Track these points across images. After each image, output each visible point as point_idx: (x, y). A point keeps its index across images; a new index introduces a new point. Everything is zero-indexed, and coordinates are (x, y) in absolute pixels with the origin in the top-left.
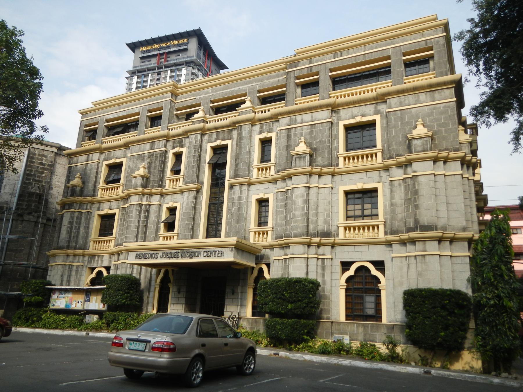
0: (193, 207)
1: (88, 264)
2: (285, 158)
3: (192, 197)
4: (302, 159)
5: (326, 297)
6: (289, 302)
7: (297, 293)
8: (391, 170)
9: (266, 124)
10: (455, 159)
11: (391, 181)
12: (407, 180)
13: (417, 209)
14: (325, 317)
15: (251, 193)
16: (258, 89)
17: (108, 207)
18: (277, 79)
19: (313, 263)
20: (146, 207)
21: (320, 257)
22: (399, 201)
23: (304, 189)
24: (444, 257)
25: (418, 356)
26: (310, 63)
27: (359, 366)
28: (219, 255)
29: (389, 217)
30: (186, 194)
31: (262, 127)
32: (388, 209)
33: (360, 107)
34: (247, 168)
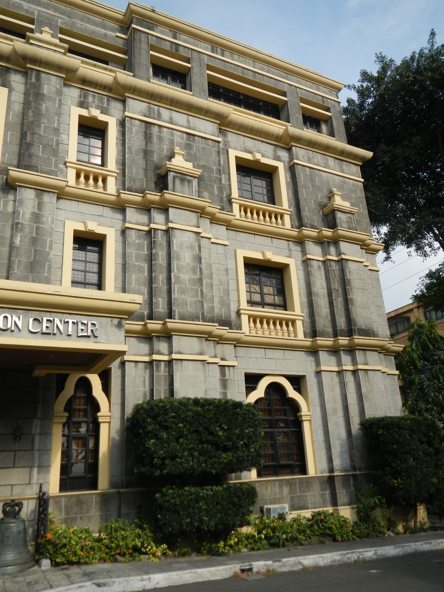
2: (141, 171)
4: (186, 183)
18: (104, 31)
26: (175, 37)
27: (388, 555)
31: (85, 97)
33: (256, 141)
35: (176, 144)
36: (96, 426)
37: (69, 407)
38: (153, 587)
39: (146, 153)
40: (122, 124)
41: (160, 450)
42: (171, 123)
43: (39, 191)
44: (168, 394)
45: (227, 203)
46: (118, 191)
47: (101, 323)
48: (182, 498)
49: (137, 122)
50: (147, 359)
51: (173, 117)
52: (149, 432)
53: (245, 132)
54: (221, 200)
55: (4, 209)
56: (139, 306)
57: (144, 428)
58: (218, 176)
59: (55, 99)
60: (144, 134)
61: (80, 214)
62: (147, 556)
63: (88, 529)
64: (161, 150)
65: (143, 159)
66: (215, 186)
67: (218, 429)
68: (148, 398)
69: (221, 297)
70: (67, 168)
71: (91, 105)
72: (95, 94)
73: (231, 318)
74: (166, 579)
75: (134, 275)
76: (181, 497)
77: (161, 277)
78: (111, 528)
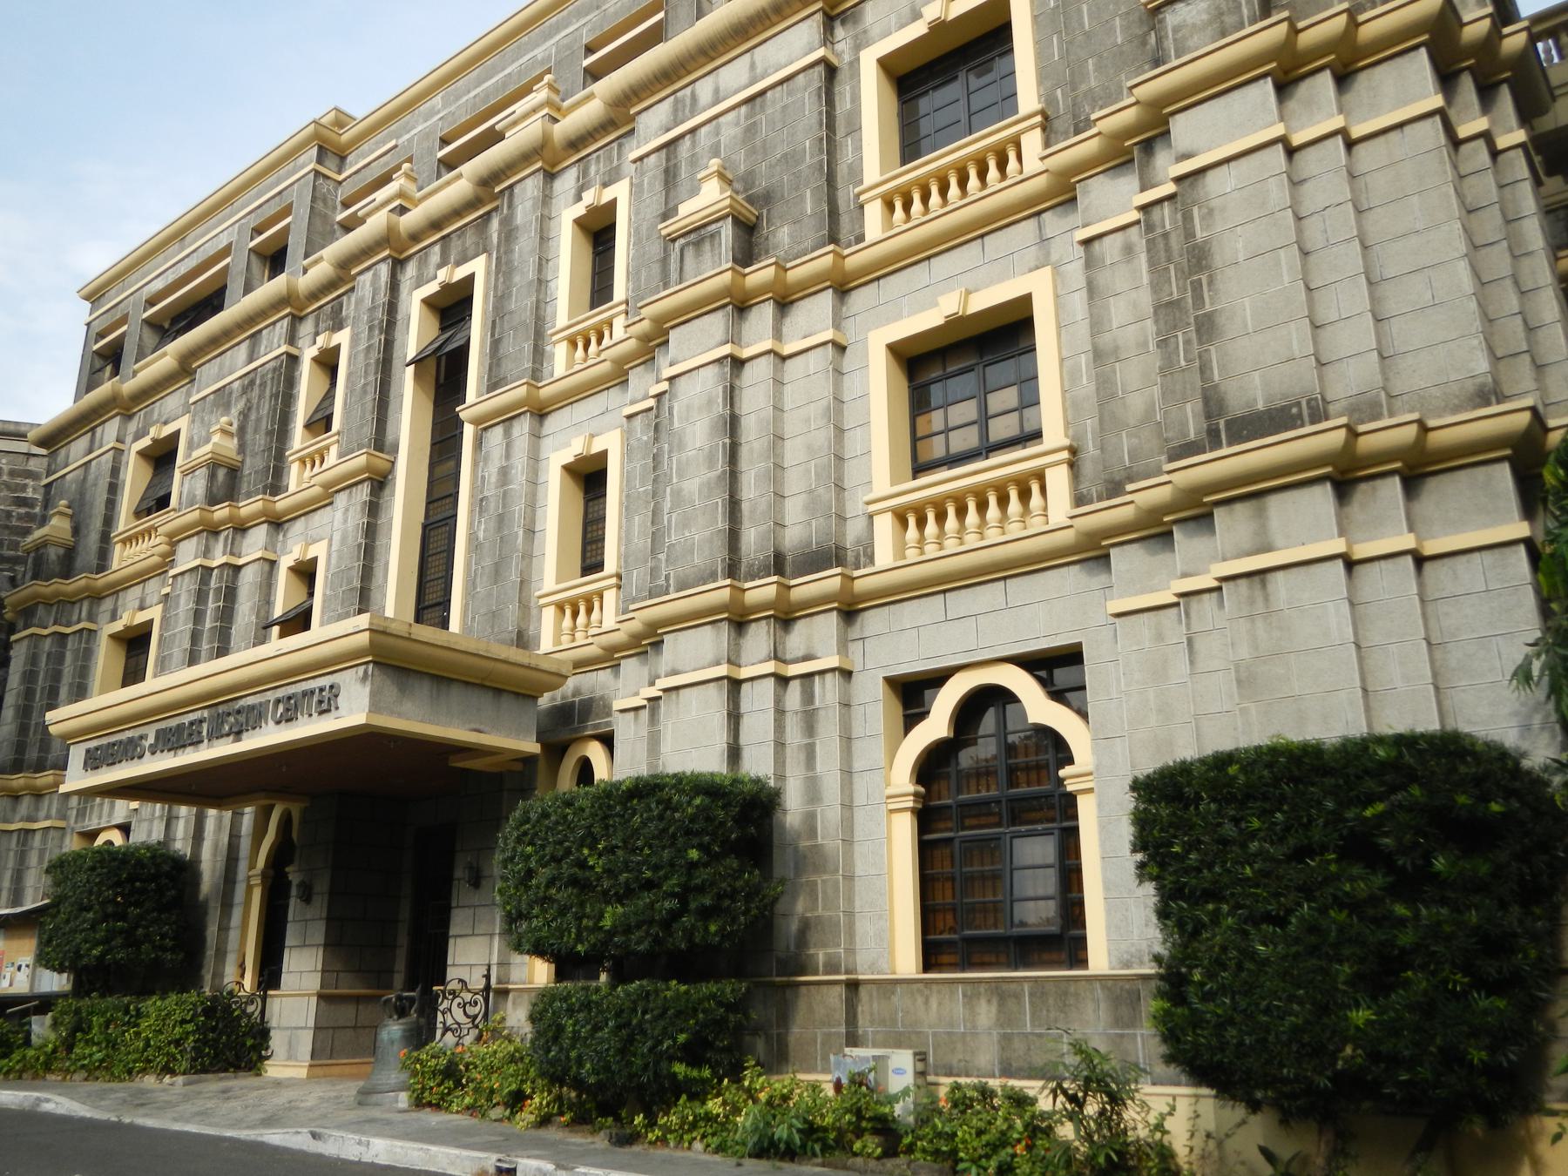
0: (359, 545)
1: (76, 822)
4: (707, 246)
5: (811, 860)
6: (606, 898)
7: (633, 851)
8: (1086, 193)
10: (1393, 46)
11: (1087, 242)
12: (1156, 213)
13: (1210, 340)
14: (821, 958)
15: (546, 443)
16: (584, 41)
19: (756, 701)
21: (793, 670)
22: (1133, 326)
23: (713, 370)
24: (1376, 565)
25: (1257, 1151)
28: (324, 706)
29: (1090, 424)
31: (585, 173)
32: (1087, 385)
34: (528, 346)
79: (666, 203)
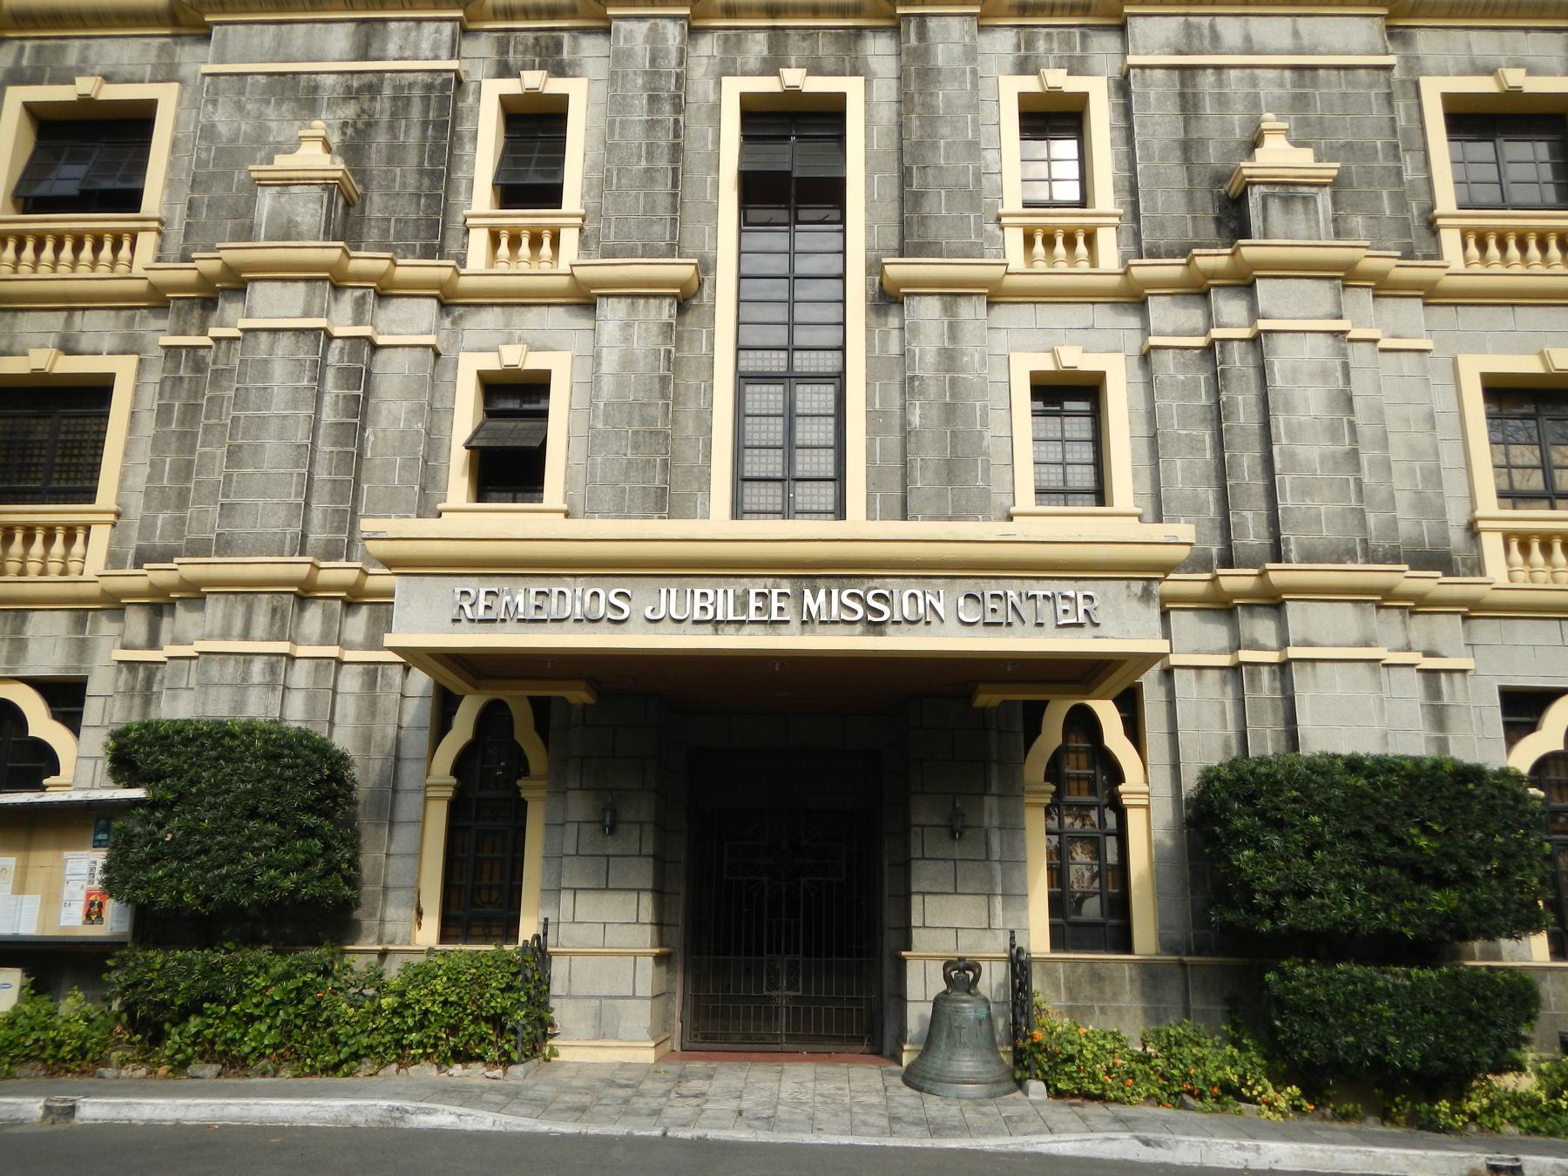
2: (1179, 198)
3: (654, 329)
4: (1298, 207)
9: (1049, 35)
17: (52, 339)
20: (355, 354)
30: (612, 312)
31: (1030, 44)
33: (1507, 35)
35: (1267, 103)
36: (1121, 813)
37: (1054, 771)
38: (1267, 1168)
39: (1188, 148)
40: (1122, 87)
41: (1269, 874)
42: (1249, 51)
43: (949, 298)
44: (1283, 743)
45: (1424, 233)
46: (1124, 261)
47: (1105, 594)
48: (1331, 987)
49: (1159, 73)
50: (1225, 660)
51: (1253, 32)
52: (1237, 833)
53: (1470, 17)
54: (1405, 228)
55: (881, 351)
56: (1189, 548)
57: (1225, 823)
58: (1391, 164)
59: (964, 73)
60: (1178, 100)
61: (1041, 332)
62: (1255, 1107)
63: (1119, 1033)
64: (1226, 131)
65: (1181, 165)
66: (1385, 194)
67: (1414, 831)
68: (1235, 752)
69: (1417, 492)
70: (1002, 229)
71: (1044, 61)
72: (1051, 30)
73: (1449, 545)
74: (1296, 1155)
75: (1178, 462)
76: (1327, 984)
77: (1246, 461)
78: (1169, 1036)
79: (1186, 131)
